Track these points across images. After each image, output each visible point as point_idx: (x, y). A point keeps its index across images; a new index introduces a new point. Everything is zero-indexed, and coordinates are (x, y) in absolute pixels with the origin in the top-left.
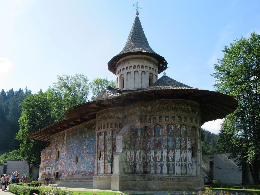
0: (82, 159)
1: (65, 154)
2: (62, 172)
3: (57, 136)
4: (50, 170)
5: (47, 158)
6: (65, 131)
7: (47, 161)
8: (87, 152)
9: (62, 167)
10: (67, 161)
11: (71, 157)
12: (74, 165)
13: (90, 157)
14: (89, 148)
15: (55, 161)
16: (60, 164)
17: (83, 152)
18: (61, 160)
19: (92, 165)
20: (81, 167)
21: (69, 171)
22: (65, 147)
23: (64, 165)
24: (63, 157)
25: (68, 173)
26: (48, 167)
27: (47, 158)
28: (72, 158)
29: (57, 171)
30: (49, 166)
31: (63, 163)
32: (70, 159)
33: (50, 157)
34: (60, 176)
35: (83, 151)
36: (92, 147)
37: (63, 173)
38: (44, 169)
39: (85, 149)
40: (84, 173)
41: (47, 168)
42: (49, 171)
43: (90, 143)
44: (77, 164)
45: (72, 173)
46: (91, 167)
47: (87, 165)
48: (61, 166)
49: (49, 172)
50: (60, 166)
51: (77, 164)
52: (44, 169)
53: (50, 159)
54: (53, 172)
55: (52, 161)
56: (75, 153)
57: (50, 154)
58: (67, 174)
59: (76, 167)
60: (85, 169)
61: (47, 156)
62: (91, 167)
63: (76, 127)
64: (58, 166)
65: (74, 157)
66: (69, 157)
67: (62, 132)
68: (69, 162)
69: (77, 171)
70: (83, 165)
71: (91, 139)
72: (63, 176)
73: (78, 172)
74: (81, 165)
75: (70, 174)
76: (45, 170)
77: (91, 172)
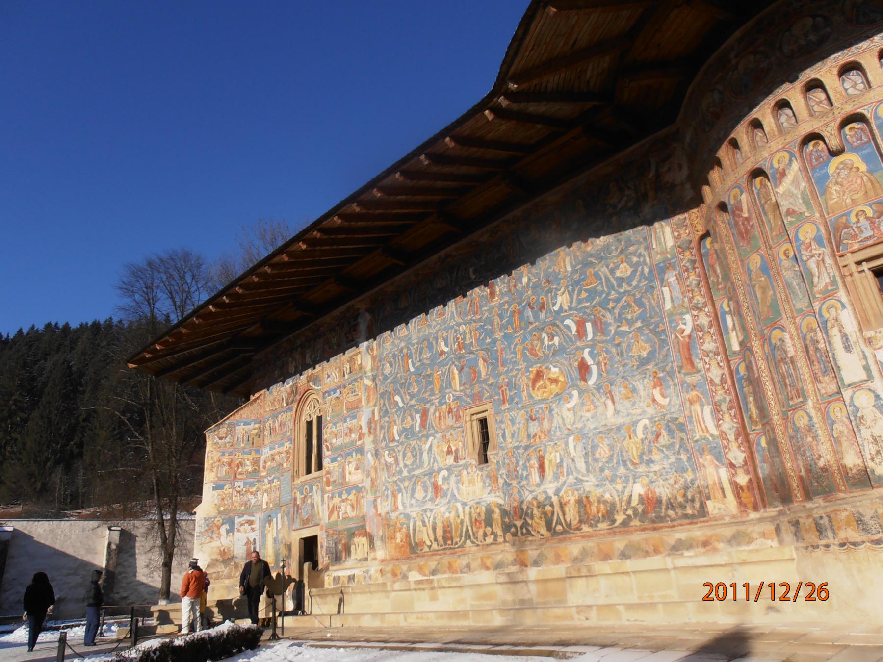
0: (531, 423)
1: (363, 422)
2: (352, 534)
3: (298, 342)
4: (253, 530)
5: (241, 464)
6: (360, 303)
7: (237, 484)
8: (584, 369)
9: (343, 501)
10: (390, 460)
11: (423, 425)
12: (459, 474)
13: (618, 391)
14: (600, 327)
15: (288, 476)
16: (328, 489)
17: (539, 375)
18: (334, 460)
19: (664, 439)
20: (535, 477)
21: (407, 517)
22: (368, 382)
23: (359, 490)
24: (353, 442)
25: (399, 536)
26: (246, 517)
27: (241, 464)
28: (427, 437)
29: (307, 533)
30: (248, 509)
31: (354, 477)
32: (413, 443)
33: (256, 462)
34: (337, 558)
35: (534, 369)
36: (630, 323)
37: (361, 541)
38: (223, 530)
39: (558, 352)
40: (572, 514)
41: (238, 520)
42: (252, 536)
43: (603, 304)
44: (484, 459)
45: (447, 530)
46: (656, 456)
47: (603, 452)
48: (337, 500)
49: (248, 543)
50: (332, 498)
51: (484, 459)
52: (223, 530)
53: (256, 471)
54: (275, 540)
55: (270, 482)
56: (457, 398)
57: (254, 442)
58: (392, 538)
59: (480, 485)
60: (579, 481)
61: (238, 458)
62: (656, 456)
63: (442, 253)
64: (317, 498)
65: (450, 421)
66: (404, 432)
67: (336, 313)
68: (409, 463)
69: (489, 512)
70: (552, 457)
71: (612, 271)
72: (360, 555)
73: (504, 513)
74: (534, 462)
75: (425, 535)
76: (228, 531)
77: (663, 491)
